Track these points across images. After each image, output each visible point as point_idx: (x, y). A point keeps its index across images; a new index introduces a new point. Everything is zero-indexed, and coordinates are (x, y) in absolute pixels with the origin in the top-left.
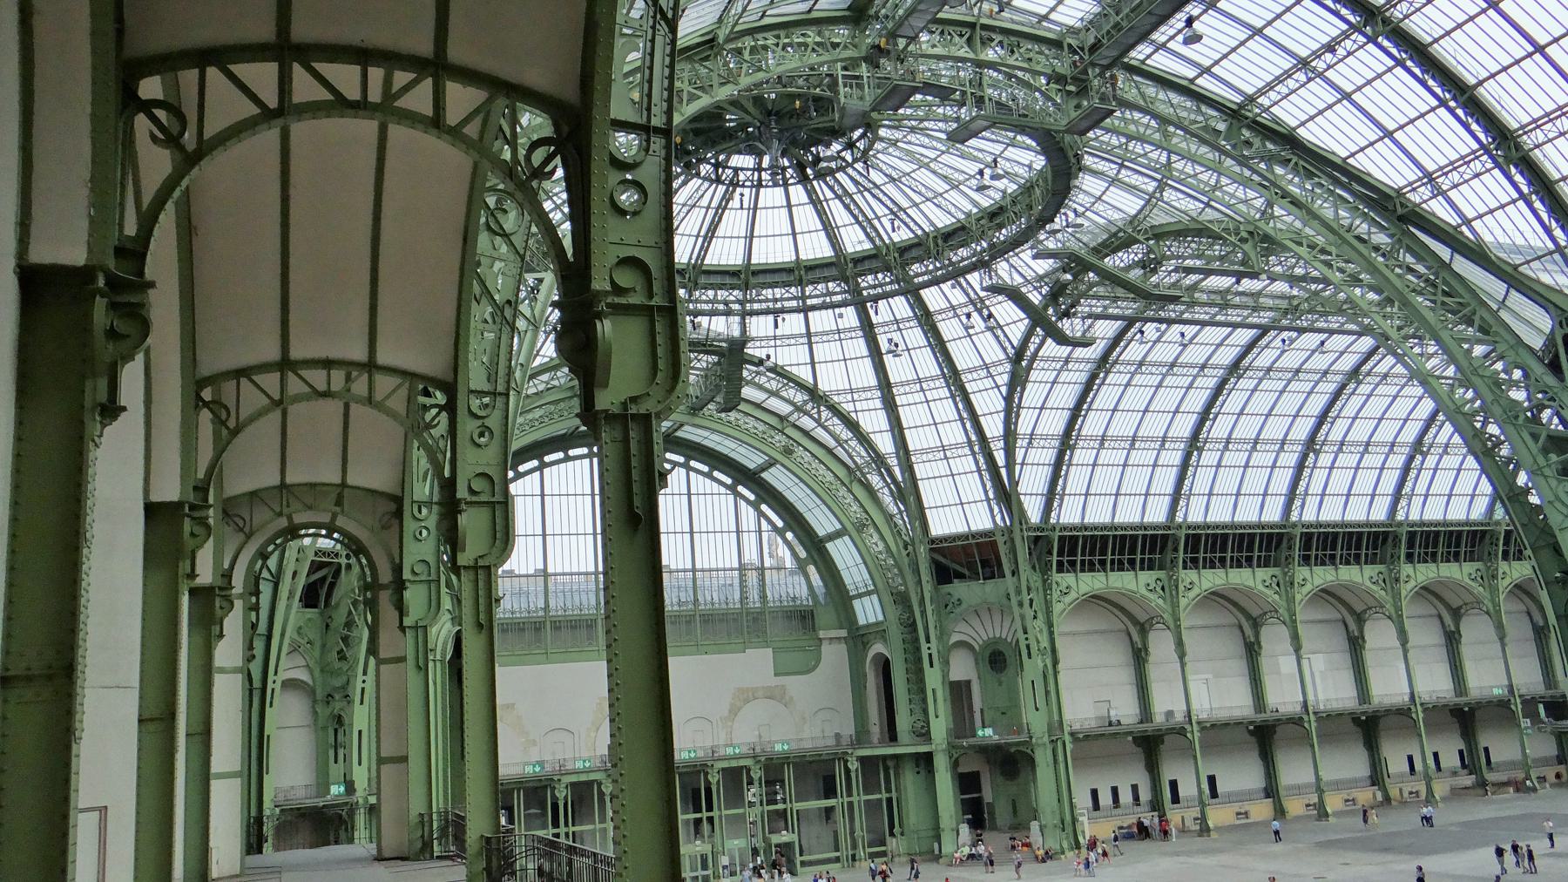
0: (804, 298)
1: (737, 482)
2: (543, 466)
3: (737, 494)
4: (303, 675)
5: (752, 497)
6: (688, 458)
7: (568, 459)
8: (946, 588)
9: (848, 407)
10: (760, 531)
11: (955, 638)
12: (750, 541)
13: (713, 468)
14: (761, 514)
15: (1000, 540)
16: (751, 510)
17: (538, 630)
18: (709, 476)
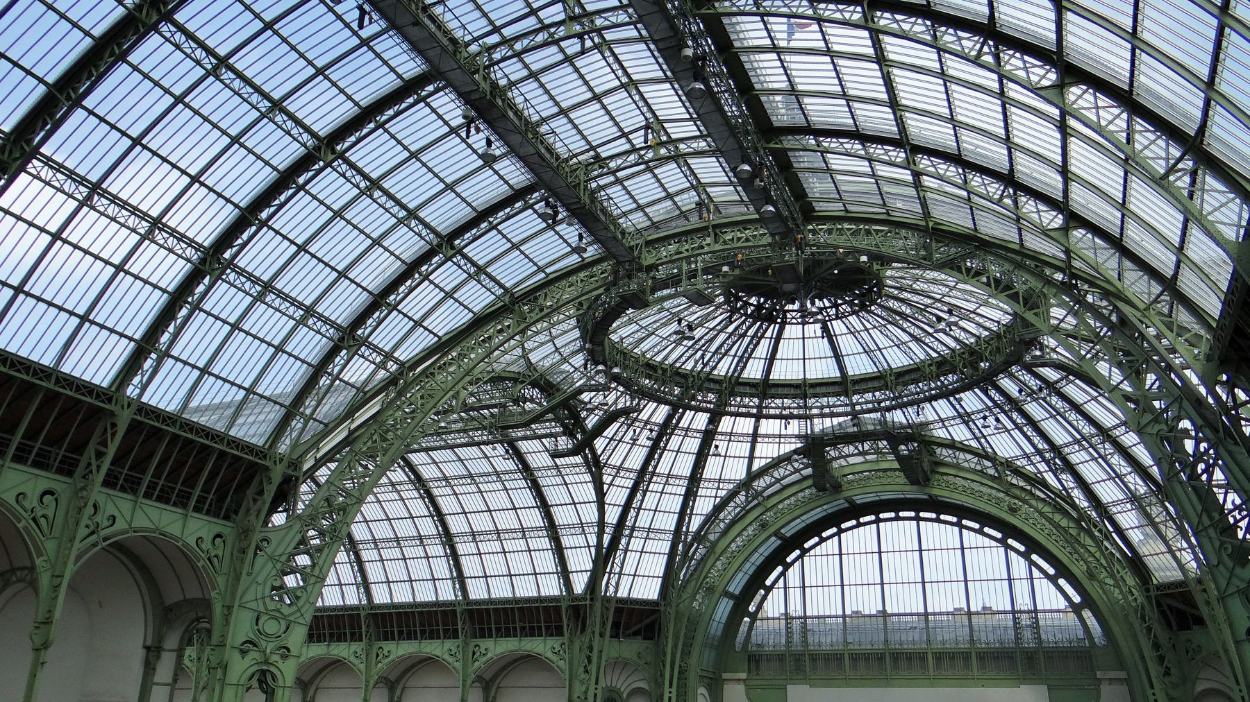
0: (806, 407)
1: (1006, 536)
2: (838, 534)
3: (1008, 547)
4: (643, 685)
5: (1022, 549)
6: (960, 518)
7: (859, 525)
8: (1185, 635)
9: (1030, 468)
10: (1032, 579)
11: (1200, 687)
12: (1022, 588)
13: (983, 525)
14: (1032, 563)
15: (1195, 589)
16: (1022, 560)
17: (953, 658)
18: (980, 532)
